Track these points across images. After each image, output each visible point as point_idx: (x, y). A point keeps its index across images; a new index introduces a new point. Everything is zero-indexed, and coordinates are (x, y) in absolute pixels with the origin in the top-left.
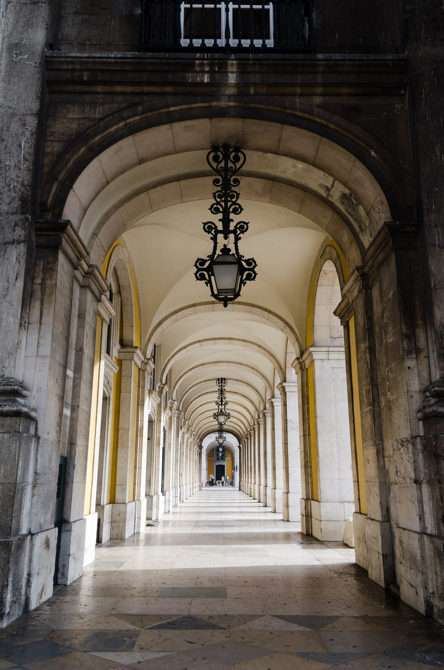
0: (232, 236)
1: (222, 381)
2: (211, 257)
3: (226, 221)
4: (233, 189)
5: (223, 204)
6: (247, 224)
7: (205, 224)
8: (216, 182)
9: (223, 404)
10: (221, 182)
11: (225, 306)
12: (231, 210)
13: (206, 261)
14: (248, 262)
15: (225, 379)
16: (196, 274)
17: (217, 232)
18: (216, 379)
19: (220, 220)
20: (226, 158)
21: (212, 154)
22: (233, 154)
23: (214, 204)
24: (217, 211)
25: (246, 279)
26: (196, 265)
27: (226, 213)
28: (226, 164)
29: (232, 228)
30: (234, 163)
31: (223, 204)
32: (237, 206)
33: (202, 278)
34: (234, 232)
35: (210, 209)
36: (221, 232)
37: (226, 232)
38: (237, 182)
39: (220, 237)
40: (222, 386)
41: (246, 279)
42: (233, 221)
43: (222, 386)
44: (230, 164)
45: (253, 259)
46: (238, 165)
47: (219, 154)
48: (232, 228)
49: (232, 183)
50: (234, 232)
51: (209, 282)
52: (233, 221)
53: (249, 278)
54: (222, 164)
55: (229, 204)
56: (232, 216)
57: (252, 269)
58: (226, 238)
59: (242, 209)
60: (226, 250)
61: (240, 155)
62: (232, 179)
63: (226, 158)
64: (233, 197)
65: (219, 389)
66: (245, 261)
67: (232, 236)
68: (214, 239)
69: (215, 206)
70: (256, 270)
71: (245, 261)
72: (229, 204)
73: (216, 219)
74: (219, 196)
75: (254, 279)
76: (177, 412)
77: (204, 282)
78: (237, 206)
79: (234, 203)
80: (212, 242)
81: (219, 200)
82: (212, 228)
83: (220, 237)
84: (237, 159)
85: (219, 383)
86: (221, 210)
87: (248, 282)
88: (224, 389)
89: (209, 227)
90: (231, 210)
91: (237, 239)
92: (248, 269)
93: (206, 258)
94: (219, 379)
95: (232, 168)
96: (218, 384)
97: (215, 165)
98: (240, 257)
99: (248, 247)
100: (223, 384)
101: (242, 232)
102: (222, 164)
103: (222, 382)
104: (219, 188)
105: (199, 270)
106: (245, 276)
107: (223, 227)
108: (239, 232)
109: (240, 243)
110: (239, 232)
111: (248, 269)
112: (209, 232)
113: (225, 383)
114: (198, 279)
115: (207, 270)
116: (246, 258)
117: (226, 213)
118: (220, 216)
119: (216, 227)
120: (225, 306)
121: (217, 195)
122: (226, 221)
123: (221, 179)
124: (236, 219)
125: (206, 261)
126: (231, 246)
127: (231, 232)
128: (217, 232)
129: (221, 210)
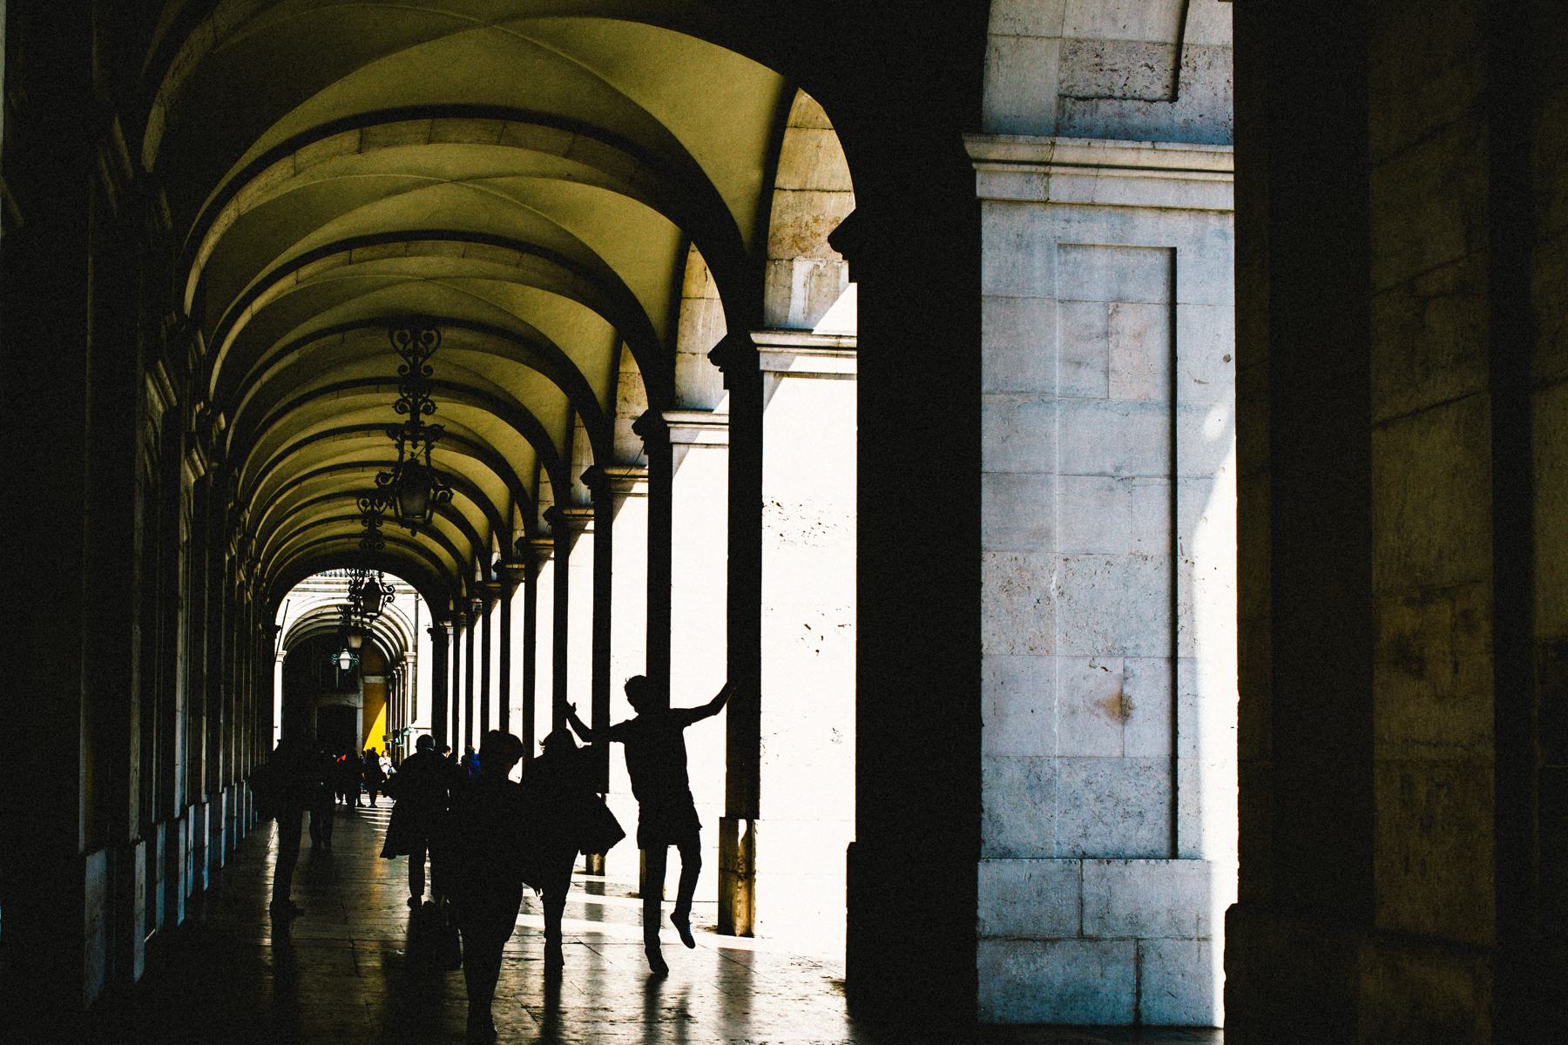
28: (415, 345)
39: (408, 443)
54: (411, 346)
58: (415, 446)
60: (414, 461)
79: (425, 400)
83: (408, 443)
96: (401, 347)
100: (421, 345)
102: (411, 346)
113: (430, 339)
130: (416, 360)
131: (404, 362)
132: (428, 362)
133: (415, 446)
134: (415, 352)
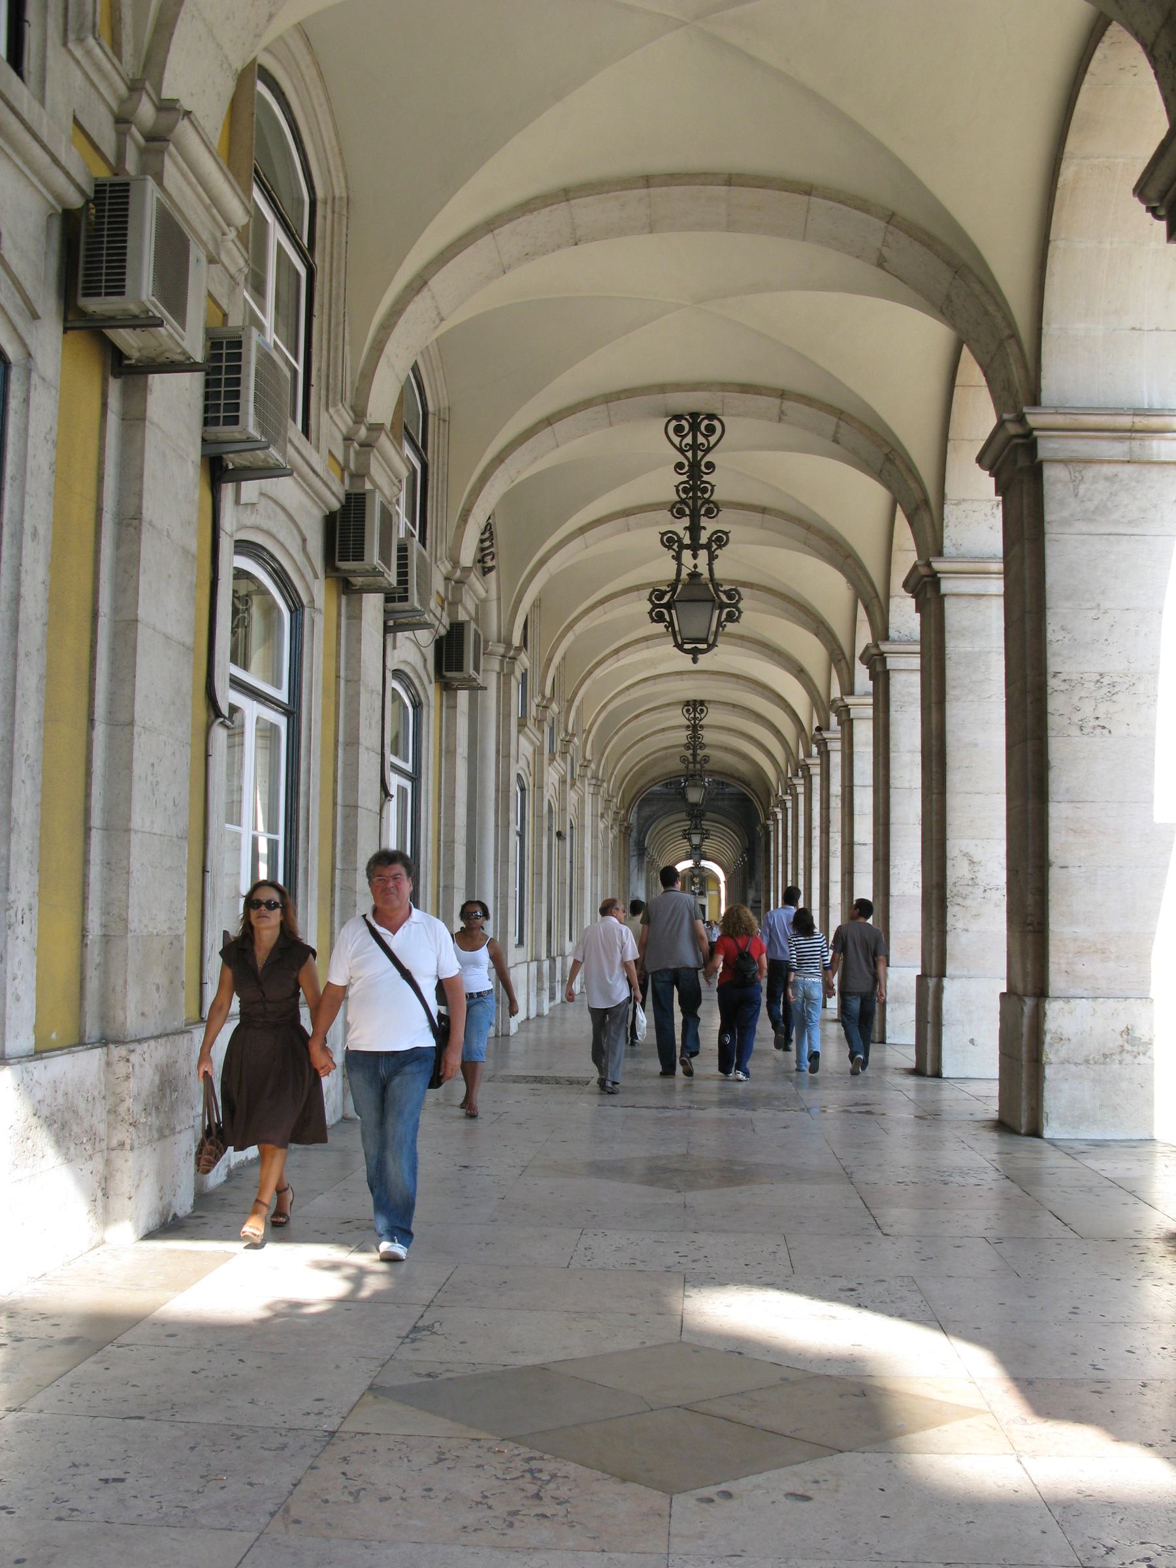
0: (703, 554)
1: (695, 706)
2: (673, 586)
3: (694, 529)
4: (705, 478)
5: (690, 502)
6: (726, 534)
7: (663, 534)
8: (679, 466)
9: (699, 758)
10: (686, 468)
11: (695, 661)
12: (703, 512)
13: (664, 593)
14: (729, 594)
15: (702, 703)
16: (650, 613)
17: (682, 547)
18: (679, 703)
19: (686, 528)
20: (694, 428)
21: (674, 423)
22: (706, 422)
23: (677, 502)
24: (681, 514)
25: (726, 620)
26: (650, 600)
27: (695, 517)
28: (695, 438)
29: (703, 540)
30: (706, 437)
31: (690, 502)
32: (711, 505)
33: (660, 618)
34: (707, 547)
35: (671, 511)
36: (687, 547)
37: (695, 547)
38: (710, 466)
39: (687, 555)
40: (695, 718)
41: (726, 620)
42: (704, 528)
43: (695, 718)
44: (701, 439)
45: (735, 590)
46: (713, 440)
47: (684, 422)
48: (703, 540)
49: (703, 468)
50: (707, 547)
51: (671, 624)
52: (704, 528)
53: (731, 618)
55: (700, 502)
56: (704, 521)
57: (735, 606)
58: (695, 556)
59: (719, 511)
60: (694, 575)
61: (716, 423)
62: (703, 463)
63: (694, 428)
64: (704, 490)
65: (688, 727)
66: (724, 592)
67: (703, 554)
68: (678, 558)
69: (678, 506)
70: (740, 605)
71: (724, 592)
72: (700, 502)
73: (680, 526)
74: (685, 491)
75: (737, 620)
76: (594, 782)
77: (662, 624)
78: (711, 505)
79: (707, 501)
80: (674, 562)
81: (684, 496)
82: (675, 542)
83: (687, 555)
84: (711, 430)
85: (688, 711)
86: (688, 512)
87: (728, 624)
88: (702, 727)
89: (669, 541)
90: (703, 512)
91: (712, 557)
92: (728, 606)
93: (663, 588)
94: (687, 703)
95: (703, 444)
97: (677, 440)
98: (717, 586)
99: (728, 566)
101: (720, 547)
102: (689, 440)
103: (695, 710)
104: (684, 478)
105: (655, 606)
106: (724, 616)
107: (691, 538)
108: (715, 546)
109: (716, 563)
110: (715, 546)
111: (728, 606)
112: (669, 548)
113: (702, 711)
114: (653, 621)
115: (668, 606)
116: (726, 587)
117: (695, 517)
118: (686, 522)
119: (680, 540)
120: (695, 661)
121: (680, 488)
122: (694, 529)
123: (686, 463)
124: (709, 527)
125: (664, 593)
126: (703, 569)
127: (702, 547)
128: (682, 547)
129: (688, 512)
130: (695, 455)
131: (681, 459)
132: (708, 458)
133: (695, 556)
134: (695, 447)
